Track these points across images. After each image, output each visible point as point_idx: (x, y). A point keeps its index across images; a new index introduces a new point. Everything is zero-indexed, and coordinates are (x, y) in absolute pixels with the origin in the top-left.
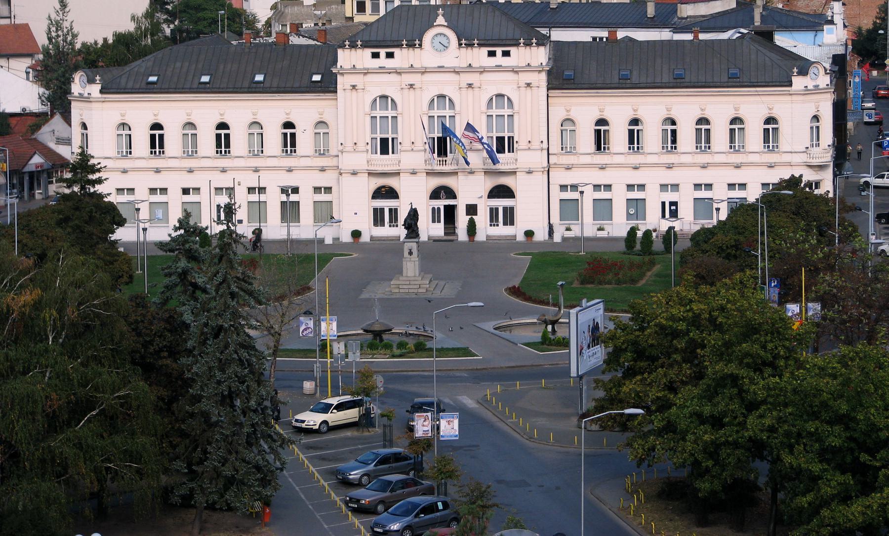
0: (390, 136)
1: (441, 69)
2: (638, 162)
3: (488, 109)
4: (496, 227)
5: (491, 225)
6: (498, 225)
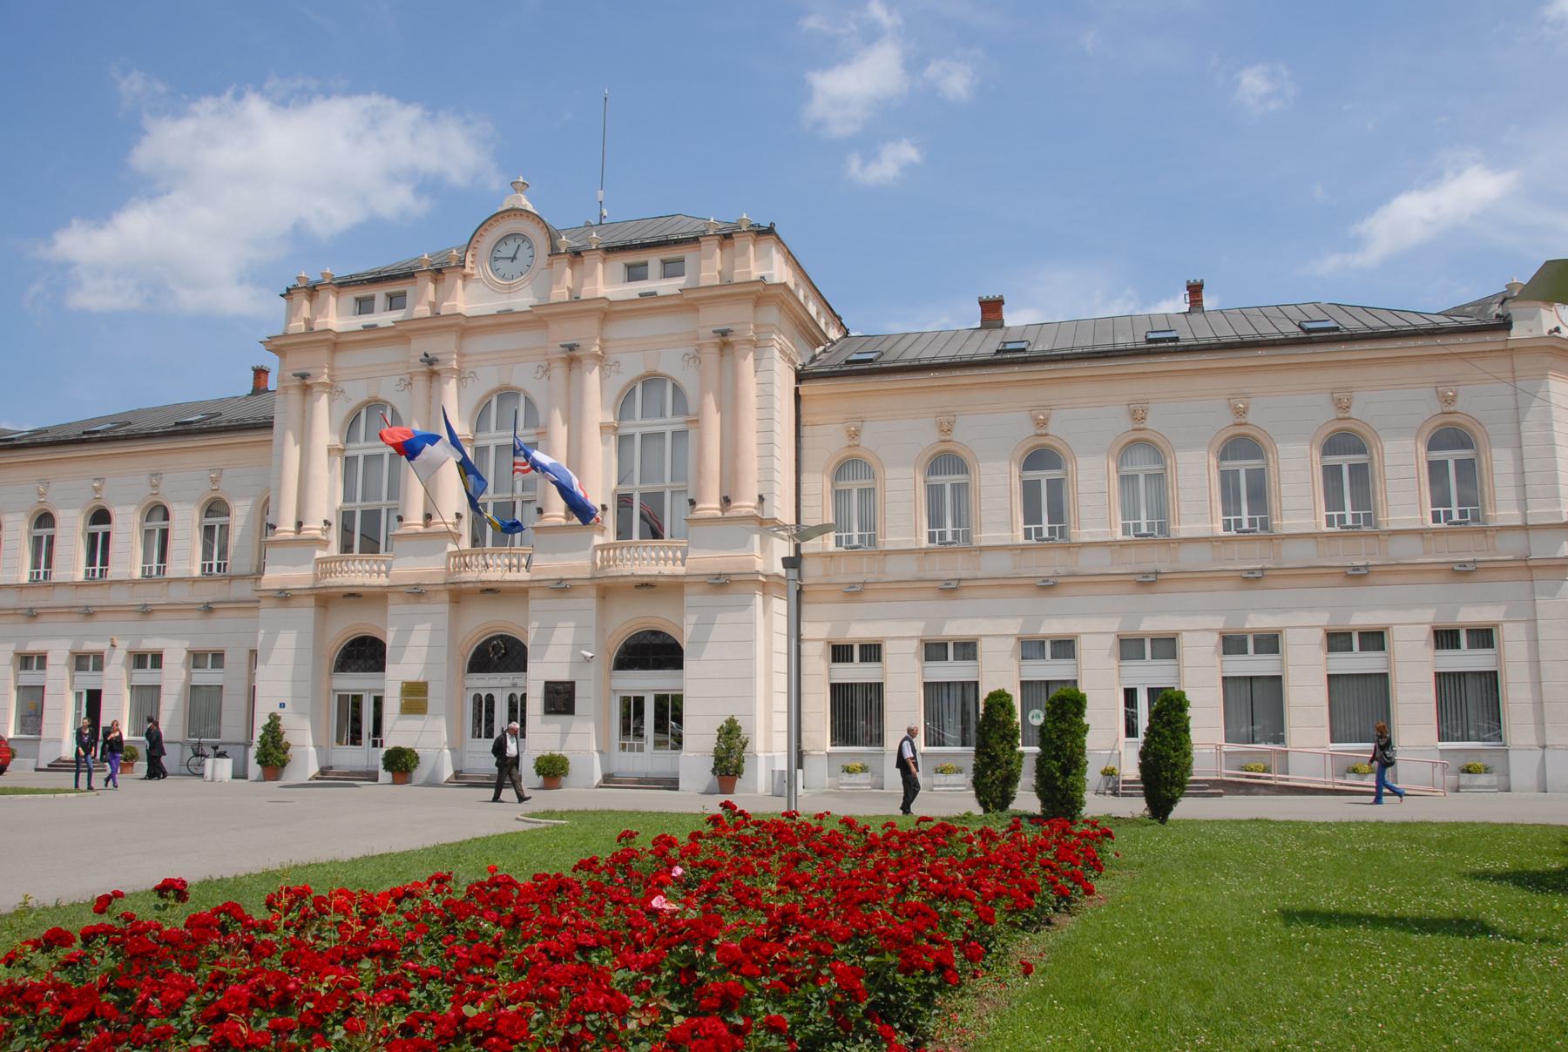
0: (383, 502)
1: (504, 322)
2: (1048, 572)
3: (621, 419)
4: (636, 754)
5: (623, 747)
6: (641, 749)
